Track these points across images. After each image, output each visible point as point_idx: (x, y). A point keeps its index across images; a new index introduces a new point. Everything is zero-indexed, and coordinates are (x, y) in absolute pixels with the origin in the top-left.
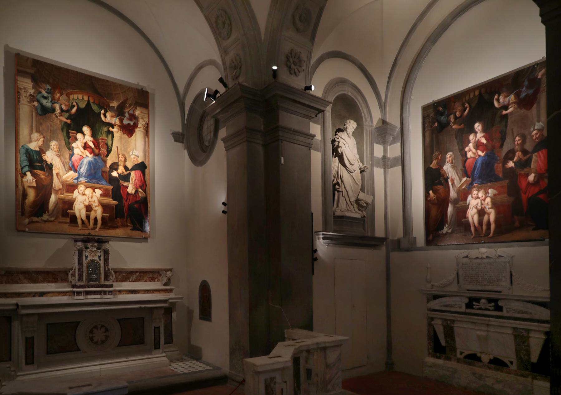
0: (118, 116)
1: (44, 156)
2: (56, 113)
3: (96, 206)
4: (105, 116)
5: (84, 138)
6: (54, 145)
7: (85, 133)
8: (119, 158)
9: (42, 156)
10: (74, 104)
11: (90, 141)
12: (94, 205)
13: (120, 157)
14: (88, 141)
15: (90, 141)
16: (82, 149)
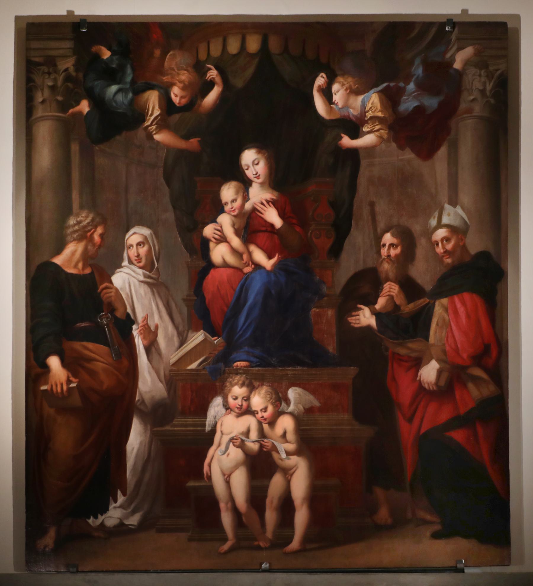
0: (377, 86)
1: (106, 288)
2: (147, 123)
3: (288, 453)
4: (327, 94)
5: (246, 198)
6: (139, 244)
7: (250, 173)
8: (379, 252)
9: (99, 290)
10: (213, 74)
11: (268, 202)
12: (282, 447)
13: (384, 245)
14: (259, 207)
15: (268, 202)
16: (236, 242)
